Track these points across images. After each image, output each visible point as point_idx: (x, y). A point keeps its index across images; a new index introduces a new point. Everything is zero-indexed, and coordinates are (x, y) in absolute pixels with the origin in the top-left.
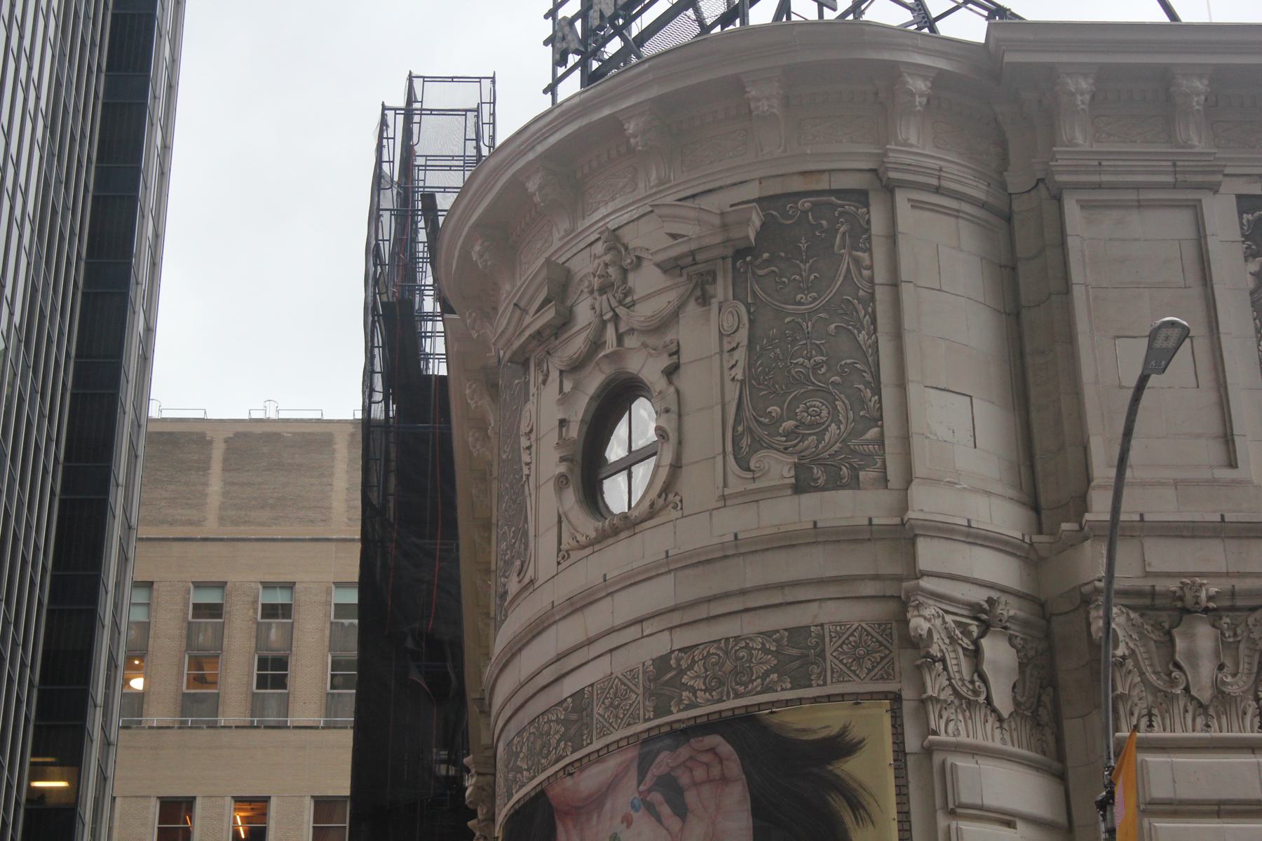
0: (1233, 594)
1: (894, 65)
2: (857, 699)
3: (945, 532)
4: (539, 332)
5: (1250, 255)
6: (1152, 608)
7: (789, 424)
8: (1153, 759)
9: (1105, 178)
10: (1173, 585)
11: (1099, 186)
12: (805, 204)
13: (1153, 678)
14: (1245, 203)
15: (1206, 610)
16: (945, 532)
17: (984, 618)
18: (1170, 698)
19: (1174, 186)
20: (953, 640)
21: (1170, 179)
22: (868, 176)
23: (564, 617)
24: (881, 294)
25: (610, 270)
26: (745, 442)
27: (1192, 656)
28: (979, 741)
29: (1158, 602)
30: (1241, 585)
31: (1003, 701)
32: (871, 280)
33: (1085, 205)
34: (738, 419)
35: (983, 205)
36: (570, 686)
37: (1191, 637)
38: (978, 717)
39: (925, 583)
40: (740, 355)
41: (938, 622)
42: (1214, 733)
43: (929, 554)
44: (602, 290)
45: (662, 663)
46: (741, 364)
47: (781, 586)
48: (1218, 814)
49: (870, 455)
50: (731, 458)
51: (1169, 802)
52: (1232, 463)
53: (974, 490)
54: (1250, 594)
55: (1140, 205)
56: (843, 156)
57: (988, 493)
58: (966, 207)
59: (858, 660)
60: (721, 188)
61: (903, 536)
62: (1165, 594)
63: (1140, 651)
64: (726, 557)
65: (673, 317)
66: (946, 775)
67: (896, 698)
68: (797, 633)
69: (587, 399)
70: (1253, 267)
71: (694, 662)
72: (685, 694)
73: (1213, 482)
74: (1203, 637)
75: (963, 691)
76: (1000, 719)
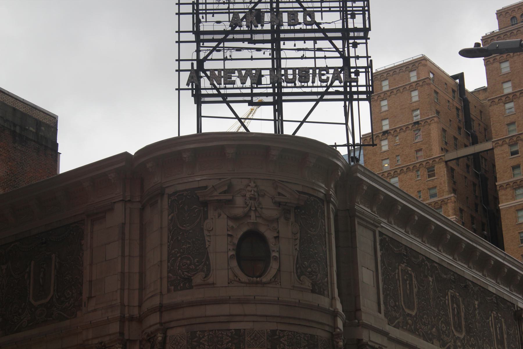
4: (220, 200)
7: (309, 269)
9: (364, 217)
21: (372, 222)
22: (323, 195)
23: (233, 303)
25: (256, 194)
26: (299, 271)
32: (325, 230)
34: (297, 263)
36: (233, 326)
40: (298, 242)
44: (251, 198)
45: (274, 332)
46: (298, 245)
47: (309, 321)
50: (296, 275)
52: (380, 312)
56: (322, 188)
60: (291, 183)
64: (295, 306)
65: (277, 220)
68: (312, 336)
69: (242, 233)
71: (284, 336)
72: (281, 345)
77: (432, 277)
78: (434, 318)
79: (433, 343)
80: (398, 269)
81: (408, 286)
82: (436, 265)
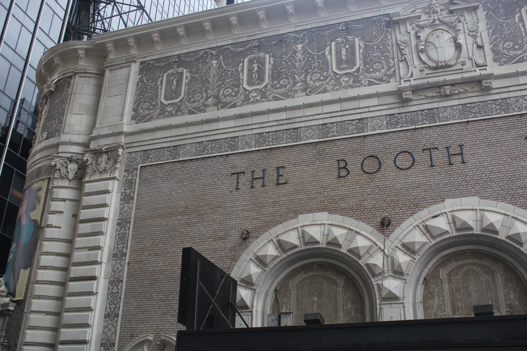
0: (110, 148)
1: (76, 49)
2: (43, 180)
3: (65, 143)
5: (140, 74)
6: (96, 153)
8: (87, 185)
10: (99, 148)
11: (113, 66)
12: (62, 81)
13: (94, 168)
14: (142, 63)
15: (105, 152)
16: (65, 143)
17: (71, 160)
18: (95, 171)
19: (127, 63)
20: (63, 165)
24: (69, 96)
27: (101, 162)
28: (63, 185)
29: (97, 152)
30: (112, 146)
31: (71, 176)
33: (110, 70)
35: (97, 74)
37: (102, 158)
38: (64, 180)
39: (60, 155)
41: (59, 162)
42: (102, 177)
43: (61, 148)
48: (97, 194)
49: (58, 130)
51: (88, 193)
53: (76, 134)
54: (113, 147)
55: (121, 68)
57: (79, 134)
58: (92, 75)
59: (46, 171)
61: (57, 145)
62: (98, 150)
63: (93, 162)
66: (52, 193)
67: (50, 178)
70: (139, 77)
73: (117, 124)
74: (105, 157)
75: (63, 175)
76: (70, 181)
77: (216, 59)
78: (213, 90)
79: (205, 112)
80: (163, 77)
81: (175, 83)
82: (226, 47)
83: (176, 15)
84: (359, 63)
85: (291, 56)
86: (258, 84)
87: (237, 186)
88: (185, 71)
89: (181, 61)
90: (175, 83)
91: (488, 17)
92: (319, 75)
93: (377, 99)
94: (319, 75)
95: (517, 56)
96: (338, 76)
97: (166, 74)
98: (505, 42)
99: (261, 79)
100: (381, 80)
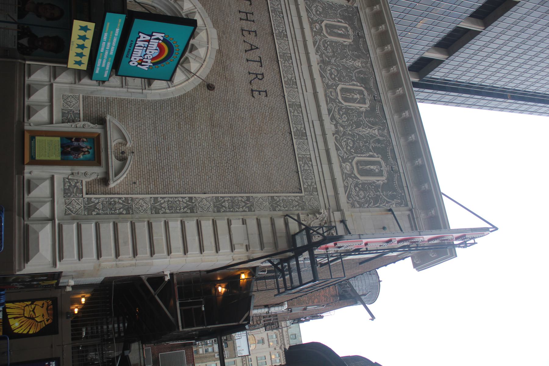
83: (398, 32)
84: (363, 179)
85: (367, 125)
86: (342, 97)
87: (250, 61)
88: (351, 41)
89: (360, 37)
90: (340, 32)
91: (341, 6)
92: (351, 145)
93: (333, 194)
94: (351, 145)
95: (312, 10)
96: (350, 161)
97: (347, 26)
98: (322, 8)
99: (346, 100)
100: (348, 197)
